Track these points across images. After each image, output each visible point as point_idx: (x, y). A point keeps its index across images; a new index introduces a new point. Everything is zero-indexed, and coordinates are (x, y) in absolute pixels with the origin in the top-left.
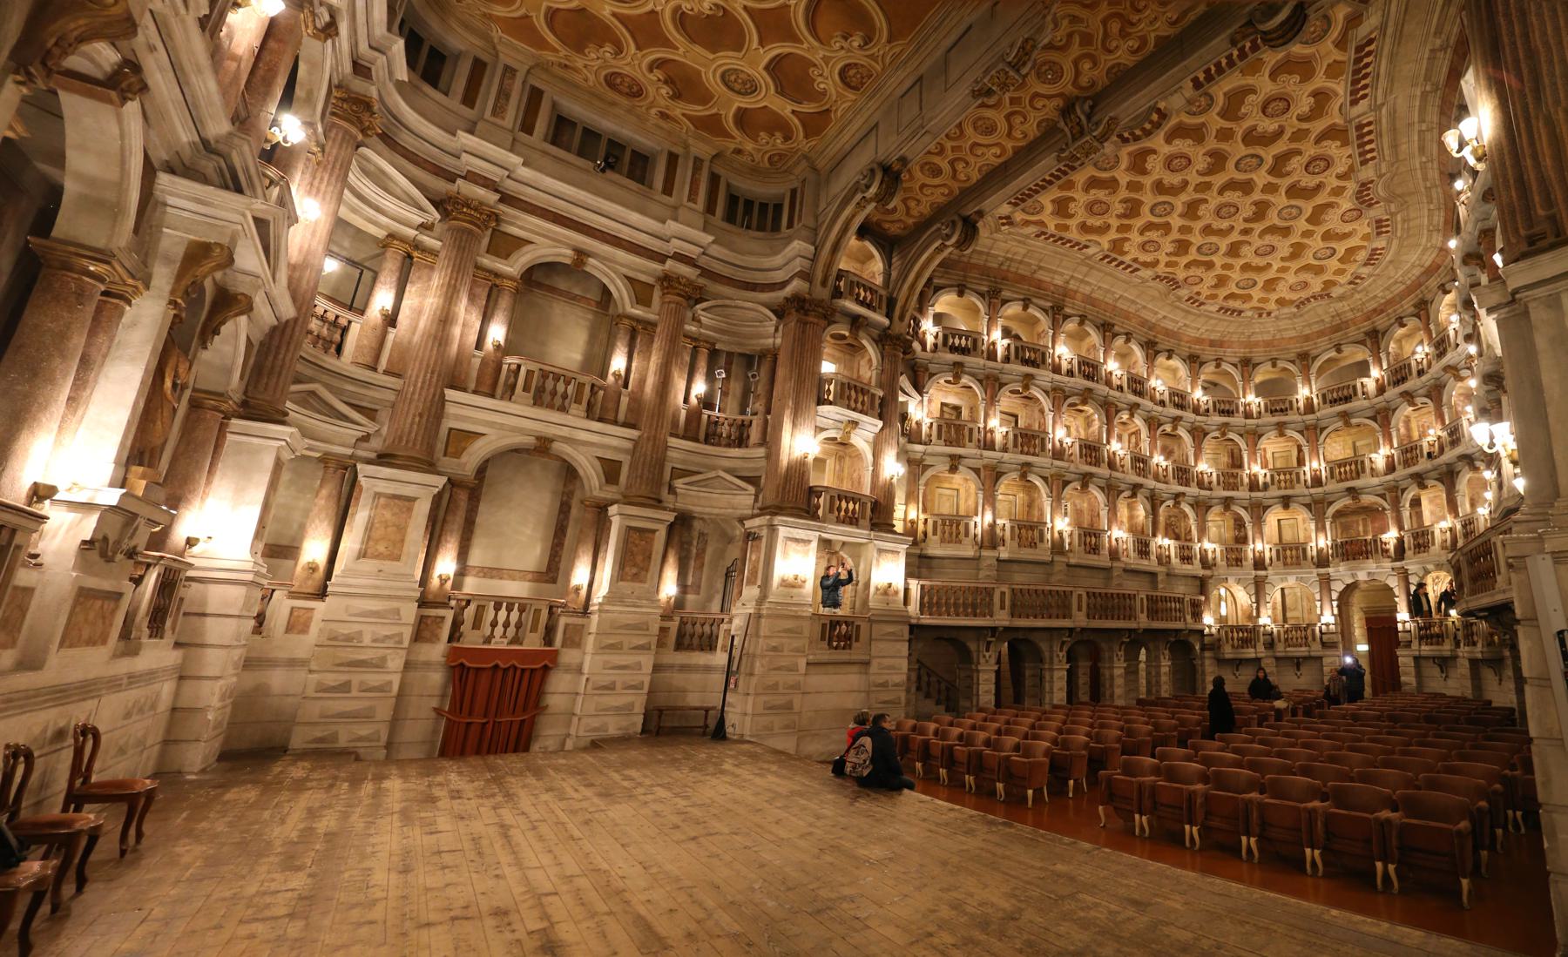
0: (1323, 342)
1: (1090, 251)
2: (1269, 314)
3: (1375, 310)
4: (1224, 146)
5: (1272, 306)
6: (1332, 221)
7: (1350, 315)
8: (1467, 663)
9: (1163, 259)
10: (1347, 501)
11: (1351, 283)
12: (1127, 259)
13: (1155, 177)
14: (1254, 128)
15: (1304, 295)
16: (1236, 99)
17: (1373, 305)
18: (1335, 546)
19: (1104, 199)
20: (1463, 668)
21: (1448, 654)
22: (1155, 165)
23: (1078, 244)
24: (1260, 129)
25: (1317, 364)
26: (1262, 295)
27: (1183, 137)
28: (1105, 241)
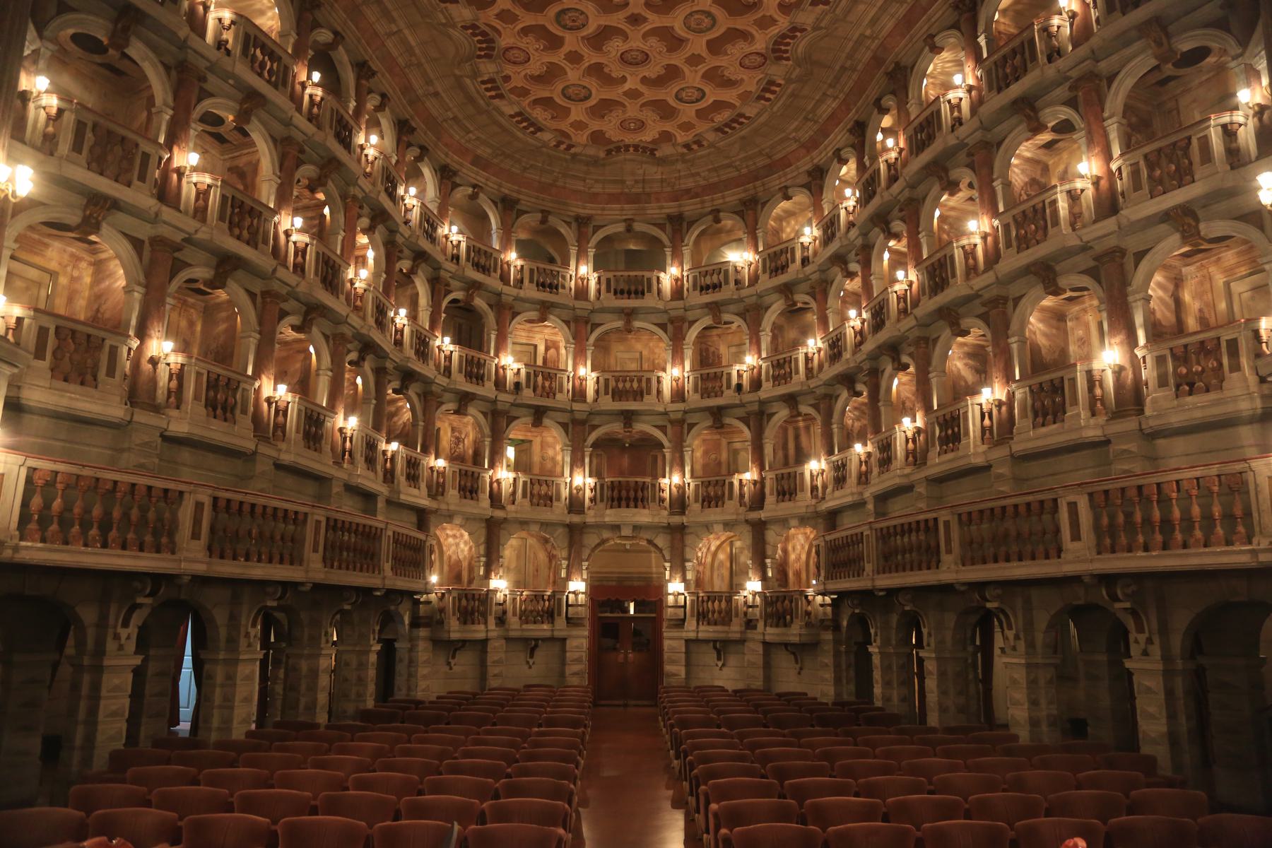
0: (614, 211)
2: (570, 147)
3: (688, 191)
5: (581, 138)
6: (729, 61)
8: (760, 649)
10: (616, 427)
11: (687, 146)
15: (630, 139)
17: (689, 183)
18: (599, 490)
20: (754, 652)
21: (737, 636)
25: (600, 235)
26: (583, 118)
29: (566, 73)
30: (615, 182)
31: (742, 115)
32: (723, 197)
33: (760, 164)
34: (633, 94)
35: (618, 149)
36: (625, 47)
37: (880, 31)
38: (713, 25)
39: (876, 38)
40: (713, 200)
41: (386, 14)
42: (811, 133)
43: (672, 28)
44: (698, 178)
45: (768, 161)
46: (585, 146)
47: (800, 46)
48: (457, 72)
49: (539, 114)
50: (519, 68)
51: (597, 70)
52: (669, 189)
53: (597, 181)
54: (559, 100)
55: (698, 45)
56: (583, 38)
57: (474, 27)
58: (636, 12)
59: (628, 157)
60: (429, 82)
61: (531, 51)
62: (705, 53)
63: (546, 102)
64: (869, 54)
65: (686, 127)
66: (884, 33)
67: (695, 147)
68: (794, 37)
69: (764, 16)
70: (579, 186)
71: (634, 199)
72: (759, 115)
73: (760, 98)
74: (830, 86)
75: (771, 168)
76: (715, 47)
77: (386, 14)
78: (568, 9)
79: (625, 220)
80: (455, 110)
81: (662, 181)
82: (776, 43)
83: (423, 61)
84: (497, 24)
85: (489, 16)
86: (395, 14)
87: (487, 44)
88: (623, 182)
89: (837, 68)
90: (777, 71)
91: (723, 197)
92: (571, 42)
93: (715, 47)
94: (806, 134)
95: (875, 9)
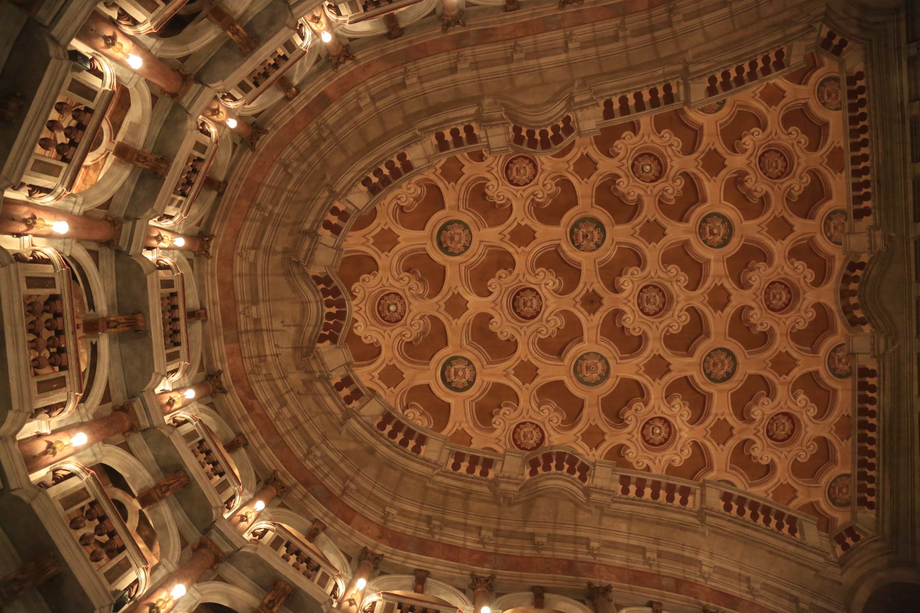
1: (699, 90)
2: (336, 230)
3: (251, 394)
4: (769, 354)
5: (357, 242)
7: (250, 349)
9: (606, 165)
11: (347, 381)
12: (646, 120)
13: (778, 260)
14: (770, 392)
16: (823, 400)
17: (263, 394)
19: (786, 182)
22: (801, 273)
23: (726, 86)
24: (764, 400)
27: (814, 323)
28: (710, 124)
29: (490, 226)
30: (254, 291)
31: (422, 440)
32: (262, 446)
33: (327, 482)
34: (456, 306)
35: (336, 292)
36: (543, 292)
37: (603, 556)
38: (588, 384)
39: (594, 555)
40: (253, 432)
41: (596, 42)
42: (410, 532)
43: (581, 341)
44: (276, 406)
45: (337, 492)
46: (338, 249)
47: (557, 480)
48: (487, 101)
49: (407, 192)
50: (498, 170)
51: (501, 260)
52: (248, 367)
53: (253, 265)
54: (438, 218)
55: (551, 371)
56: (559, 245)
57: (569, 130)
58: (604, 301)
59: (313, 307)
60: (475, 66)
61: (530, 189)
62: (539, 381)
63: (434, 199)
64: (571, 556)
65: (392, 376)
66: (605, 560)
67: (346, 392)
68: (571, 471)
69: (603, 434)
70: (245, 240)
71: (229, 321)
72: (426, 462)
73: (459, 457)
74: (497, 533)
75: (328, 498)
76: (554, 392)
77: (596, 42)
78: (603, 231)
79: (203, 308)
80: (417, 88)
81: (262, 357)
82: (561, 456)
83: (513, 66)
84: (575, 155)
85: (585, 147)
86: (592, 50)
87: (529, 141)
88: (255, 301)
89: (528, 530)
90: (513, 466)
91: (262, 446)
92: (549, 235)
93: (554, 392)
94: (399, 525)
95: (626, 541)
